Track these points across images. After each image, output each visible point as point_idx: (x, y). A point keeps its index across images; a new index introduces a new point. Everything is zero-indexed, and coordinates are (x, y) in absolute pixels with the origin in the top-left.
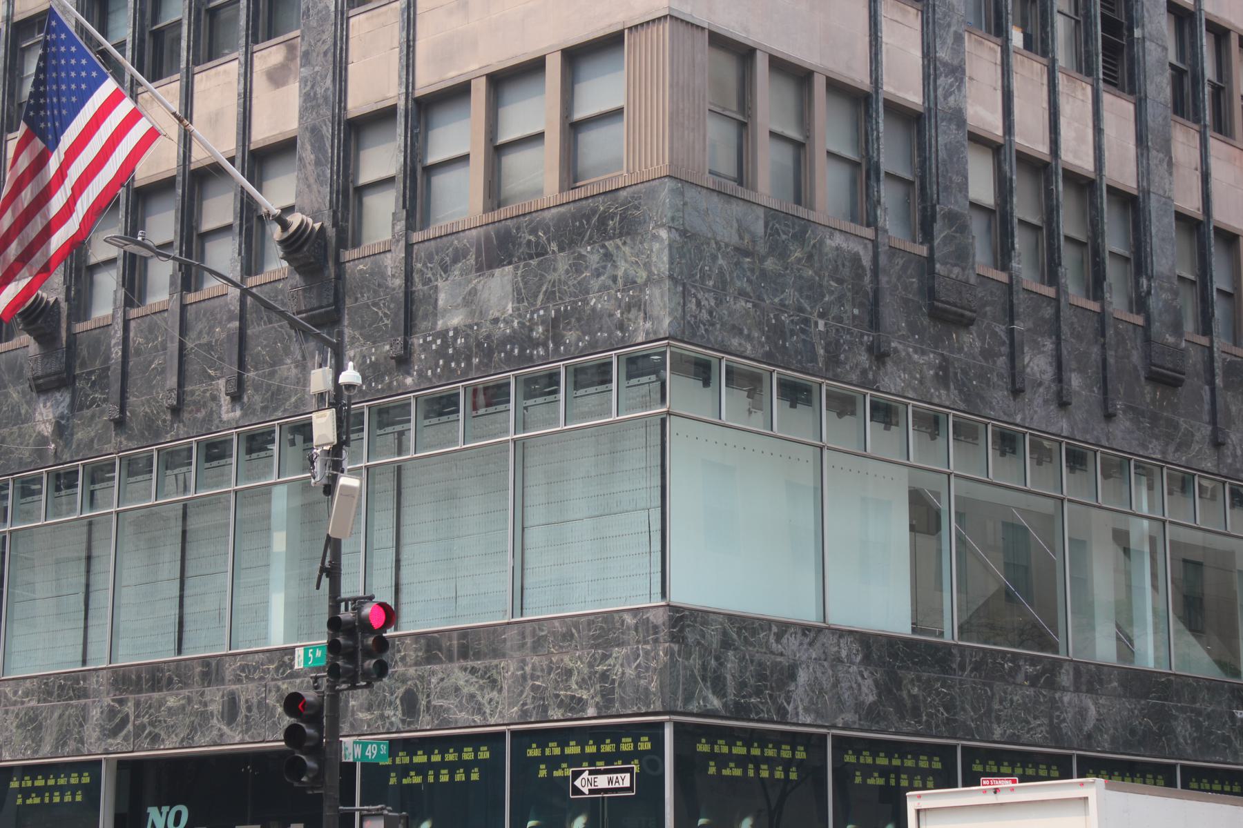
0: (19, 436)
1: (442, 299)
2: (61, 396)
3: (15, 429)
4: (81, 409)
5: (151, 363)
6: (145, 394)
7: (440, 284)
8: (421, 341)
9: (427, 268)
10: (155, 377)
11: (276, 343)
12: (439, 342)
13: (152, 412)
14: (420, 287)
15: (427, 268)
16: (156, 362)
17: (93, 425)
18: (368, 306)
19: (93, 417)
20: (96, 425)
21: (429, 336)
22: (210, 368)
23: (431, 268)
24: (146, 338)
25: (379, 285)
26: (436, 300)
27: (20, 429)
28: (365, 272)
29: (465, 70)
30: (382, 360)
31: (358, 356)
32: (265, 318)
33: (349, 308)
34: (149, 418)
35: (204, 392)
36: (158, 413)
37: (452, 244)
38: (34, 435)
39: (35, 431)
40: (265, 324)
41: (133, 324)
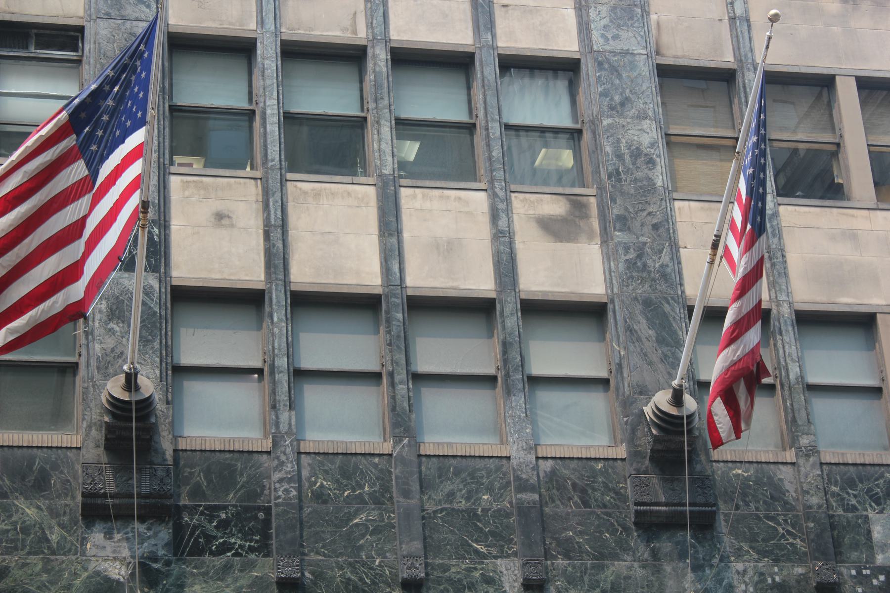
0: (45, 570)
1: (877, 533)
2: (149, 529)
3: (32, 559)
4: (197, 551)
5: (350, 517)
6: (341, 554)
7: (871, 514)
8: (854, 572)
9: (848, 493)
10: (363, 536)
11: (601, 533)
12: (882, 578)
13: (361, 579)
14: (840, 512)
15: (848, 493)
16: (363, 516)
17: (230, 580)
18: (758, 518)
19: (227, 568)
20: (236, 580)
21: (866, 568)
22: (476, 541)
23: (855, 496)
24: (337, 481)
25: (772, 497)
26: (869, 532)
27: (47, 561)
28: (748, 479)
29: (866, 302)
30: (793, 582)
31: (750, 573)
32: (576, 498)
33: (726, 515)
34: (356, 587)
35: (469, 570)
36: (373, 582)
37: (882, 476)
38: (85, 575)
39: (86, 570)
40: (575, 503)
41: (305, 460)
